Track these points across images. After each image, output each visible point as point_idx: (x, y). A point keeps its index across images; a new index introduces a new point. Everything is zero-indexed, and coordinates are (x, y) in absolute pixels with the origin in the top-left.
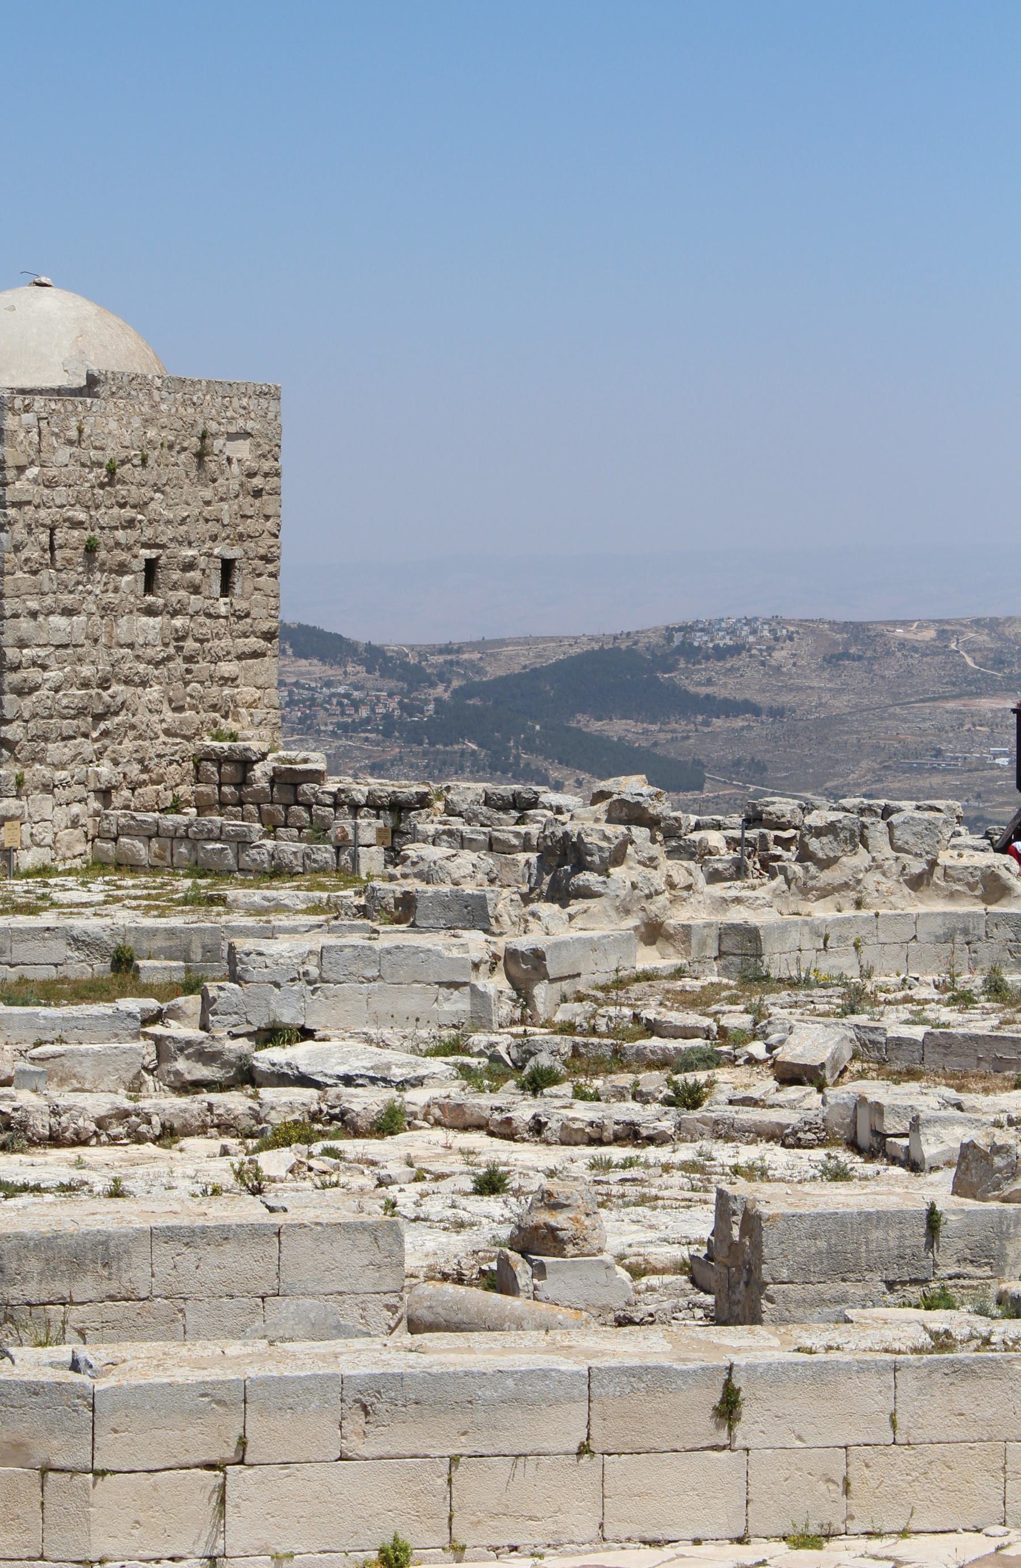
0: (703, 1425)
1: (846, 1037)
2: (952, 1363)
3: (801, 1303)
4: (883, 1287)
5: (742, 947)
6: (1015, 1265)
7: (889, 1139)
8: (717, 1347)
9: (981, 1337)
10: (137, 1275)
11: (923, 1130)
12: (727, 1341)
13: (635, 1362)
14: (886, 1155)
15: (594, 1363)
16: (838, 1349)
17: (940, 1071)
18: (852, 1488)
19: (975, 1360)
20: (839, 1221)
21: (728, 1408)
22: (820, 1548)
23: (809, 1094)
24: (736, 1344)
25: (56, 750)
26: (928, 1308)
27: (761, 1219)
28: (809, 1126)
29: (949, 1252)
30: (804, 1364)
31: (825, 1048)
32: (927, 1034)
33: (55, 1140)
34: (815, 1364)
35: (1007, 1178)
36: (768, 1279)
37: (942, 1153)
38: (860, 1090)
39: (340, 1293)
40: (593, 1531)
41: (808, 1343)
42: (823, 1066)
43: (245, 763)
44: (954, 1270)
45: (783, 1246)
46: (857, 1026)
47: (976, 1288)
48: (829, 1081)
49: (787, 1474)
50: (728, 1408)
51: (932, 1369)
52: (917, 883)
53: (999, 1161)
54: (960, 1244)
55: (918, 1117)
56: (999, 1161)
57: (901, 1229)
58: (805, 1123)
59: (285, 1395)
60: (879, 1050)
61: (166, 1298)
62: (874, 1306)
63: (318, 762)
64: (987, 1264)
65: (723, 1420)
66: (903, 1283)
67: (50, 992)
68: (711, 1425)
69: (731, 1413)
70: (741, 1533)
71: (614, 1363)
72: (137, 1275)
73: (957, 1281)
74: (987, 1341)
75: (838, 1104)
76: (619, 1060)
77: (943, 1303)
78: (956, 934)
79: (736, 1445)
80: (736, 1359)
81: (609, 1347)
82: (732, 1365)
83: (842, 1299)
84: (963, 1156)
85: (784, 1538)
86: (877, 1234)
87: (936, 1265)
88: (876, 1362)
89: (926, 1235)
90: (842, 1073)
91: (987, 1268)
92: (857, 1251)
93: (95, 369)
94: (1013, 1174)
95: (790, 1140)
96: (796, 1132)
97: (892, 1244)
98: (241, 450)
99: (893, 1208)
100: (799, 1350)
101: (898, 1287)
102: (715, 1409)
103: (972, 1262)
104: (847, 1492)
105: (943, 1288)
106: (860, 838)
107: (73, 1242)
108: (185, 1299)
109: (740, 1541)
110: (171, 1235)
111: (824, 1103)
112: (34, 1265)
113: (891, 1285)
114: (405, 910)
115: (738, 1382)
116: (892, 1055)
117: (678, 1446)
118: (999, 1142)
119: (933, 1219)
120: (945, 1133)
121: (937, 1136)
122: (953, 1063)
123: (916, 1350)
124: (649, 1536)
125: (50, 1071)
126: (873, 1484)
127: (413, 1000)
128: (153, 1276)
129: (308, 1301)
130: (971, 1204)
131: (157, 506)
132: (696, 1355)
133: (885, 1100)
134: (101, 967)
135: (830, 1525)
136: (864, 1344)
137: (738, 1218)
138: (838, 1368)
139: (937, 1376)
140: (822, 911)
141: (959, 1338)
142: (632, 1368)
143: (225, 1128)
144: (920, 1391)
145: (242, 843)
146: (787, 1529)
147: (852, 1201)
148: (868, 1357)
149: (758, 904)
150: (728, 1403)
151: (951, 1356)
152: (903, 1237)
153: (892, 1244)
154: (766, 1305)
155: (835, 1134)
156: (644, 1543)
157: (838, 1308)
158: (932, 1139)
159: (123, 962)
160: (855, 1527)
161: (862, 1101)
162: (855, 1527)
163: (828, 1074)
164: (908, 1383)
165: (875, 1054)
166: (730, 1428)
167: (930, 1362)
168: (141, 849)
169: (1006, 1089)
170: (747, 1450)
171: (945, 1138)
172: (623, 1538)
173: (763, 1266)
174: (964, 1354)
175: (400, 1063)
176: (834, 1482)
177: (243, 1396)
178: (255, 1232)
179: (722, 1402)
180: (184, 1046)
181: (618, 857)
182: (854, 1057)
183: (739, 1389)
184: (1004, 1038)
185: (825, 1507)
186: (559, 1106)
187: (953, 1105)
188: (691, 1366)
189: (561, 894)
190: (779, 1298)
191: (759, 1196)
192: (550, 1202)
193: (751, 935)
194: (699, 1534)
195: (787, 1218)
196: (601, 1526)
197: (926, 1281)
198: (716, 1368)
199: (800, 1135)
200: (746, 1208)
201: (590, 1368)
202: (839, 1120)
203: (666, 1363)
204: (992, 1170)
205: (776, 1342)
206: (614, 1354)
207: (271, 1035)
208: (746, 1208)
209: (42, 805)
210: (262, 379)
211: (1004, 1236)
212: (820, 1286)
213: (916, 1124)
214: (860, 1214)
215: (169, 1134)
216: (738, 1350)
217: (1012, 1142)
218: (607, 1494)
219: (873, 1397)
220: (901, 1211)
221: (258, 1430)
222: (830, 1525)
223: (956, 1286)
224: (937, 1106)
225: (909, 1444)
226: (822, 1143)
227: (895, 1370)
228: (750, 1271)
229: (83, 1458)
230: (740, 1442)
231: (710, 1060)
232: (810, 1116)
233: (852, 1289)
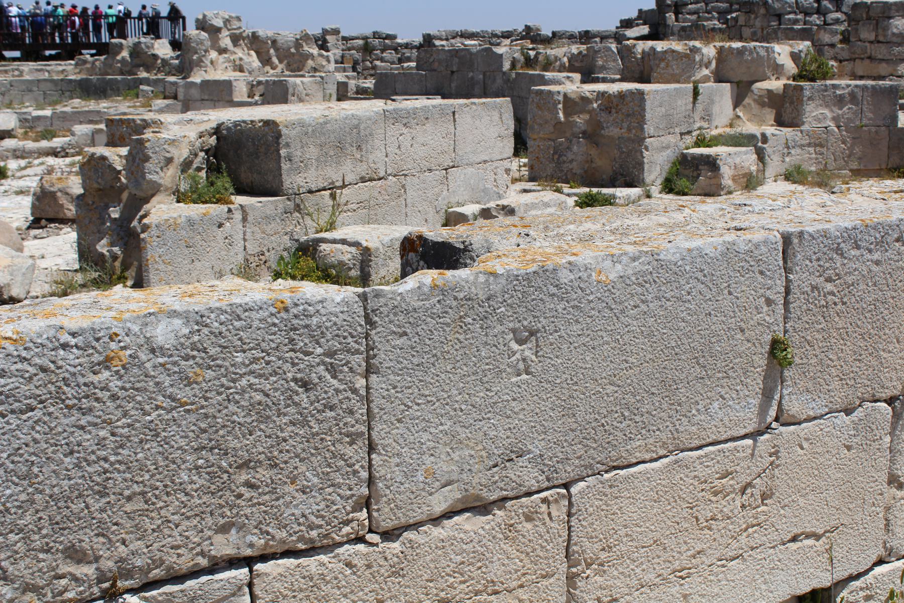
39: (485, 162)
61: (395, 176)
95: (63, 154)
107: (337, 126)
108: (405, 175)
112: (312, 152)
116: (36, 124)
128: (387, 156)
129: (470, 170)
137: (560, 106)
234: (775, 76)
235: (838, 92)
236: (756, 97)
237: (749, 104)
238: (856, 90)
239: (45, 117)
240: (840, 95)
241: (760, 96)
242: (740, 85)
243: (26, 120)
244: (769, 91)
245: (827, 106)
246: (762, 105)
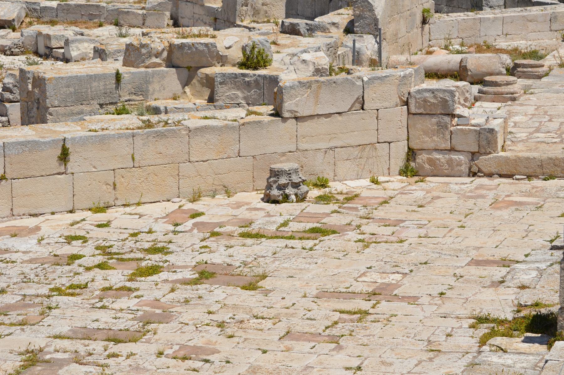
0: (54, 164)
1: (22, 7)
2: (156, 132)
3: (64, 115)
4: (98, 107)
6: (153, 94)
7: (54, 50)
8: (55, 132)
9: (164, 121)
11: (71, 45)
12: (58, 129)
13: (22, 139)
14: (53, 57)
15: (5, 140)
16: (106, 129)
17: (65, 21)
18: (116, 187)
19: (166, 131)
21: (64, 156)
22: (105, 212)
23: (9, 32)
24: (63, 130)
26: (118, 114)
27: (45, 80)
28: (17, 46)
29: (125, 90)
30: (95, 136)
31: (14, 12)
32: (59, 5)
34: (100, 136)
35: (147, 58)
36: (50, 106)
37: (80, 54)
38: (38, 29)
40: (8, 212)
41: (93, 128)
42: (14, 20)
44: (127, 98)
45: (55, 91)
46: (26, 2)
47: (135, 104)
48: (17, 27)
49: (90, 183)
50: (64, 156)
51: (148, 135)
53: (144, 51)
54: (130, 87)
55: (68, 39)
56: (144, 51)
57: (105, 82)
58: (15, 45)
60: (37, 12)
62: (95, 115)
64: (141, 94)
65: (62, 162)
66: (107, 104)
68: (57, 164)
69: (65, 158)
70: (71, 208)
71: (13, 140)
73: (129, 102)
74: (166, 123)
75: (28, 36)
77: (124, 112)
79: (68, 172)
80: (66, 135)
81: (8, 134)
82: (65, 138)
83: (81, 113)
84: (127, 49)
85: (90, 210)
86: (95, 84)
87: (120, 96)
88: (125, 134)
89: (116, 83)
90: (22, 23)
91: (141, 96)
92: (87, 92)
94: (150, 56)
96: (11, 49)
97: (101, 88)
99: (101, 73)
100: (90, 131)
101: (105, 106)
102: (59, 157)
103: (135, 94)
104: (114, 188)
105: (124, 106)
109: (71, 212)
111: (22, 35)
113: (101, 105)
115: (68, 145)
116: (43, 14)
117: (43, 174)
118: (144, 43)
119: (118, 77)
120: (81, 46)
121: (77, 47)
122: (71, 17)
123: (139, 128)
124: (33, 212)
126: (126, 184)
130: (132, 70)
132: (47, 135)
133: (51, 33)
135: (108, 202)
136: (118, 127)
137: (31, 81)
138: (109, 137)
139: (150, 138)
141: (154, 122)
142: (22, 142)
144: (144, 145)
146: (91, 206)
147: (82, 70)
148: (121, 131)
150: (64, 154)
151: (153, 129)
152: (105, 85)
153: (101, 88)
154: (49, 117)
155: (28, 49)
156: (31, 215)
157: (80, 116)
158: (75, 49)
160: (119, 203)
161: (39, 34)
162: (119, 203)
163: (16, 24)
164: (139, 141)
165: (35, 14)
166: (65, 165)
167: (148, 132)
169: (95, 27)
170: (73, 174)
171: (81, 48)
172: (21, 214)
173: (47, 100)
174: (160, 128)
176: (109, 185)
179: (61, 154)
182: (27, 16)
183: (69, 148)
184: (93, 5)
185: (108, 197)
187: (79, 34)
188: (47, 140)
190: (54, 114)
191: (40, 71)
194: (54, 210)
195: (57, 79)
196: (12, 210)
197: (116, 103)
198: (58, 140)
199: (12, 50)
200: (34, 76)
201: (4, 143)
202: (30, 43)
203: (37, 139)
204: (141, 55)
205: (79, 128)
206: (12, 137)
208: (34, 76)
211: (148, 82)
212: (72, 107)
213: (67, 42)
214: (87, 76)
216: (64, 132)
217: (149, 42)
218: (13, 196)
220: (105, 74)
222: (108, 202)
223: (128, 104)
224: (72, 34)
225: (140, 167)
226: (23, 53)
227: (133, 136)
228: (38, 103)
230: (69, 171)
232: (16, 41)
233: (84, 108)
234: (221, 64)
235: (247, 79)
236: (199, 79)
237: (194, 83)
238: (259, 78)
239: (51, 8)
240: (248, 82)
241: (201, 78)
242: (191, 69)
243: (35, 10)
244: (207, 75)
245: (238, 89)
246: (203, 85)
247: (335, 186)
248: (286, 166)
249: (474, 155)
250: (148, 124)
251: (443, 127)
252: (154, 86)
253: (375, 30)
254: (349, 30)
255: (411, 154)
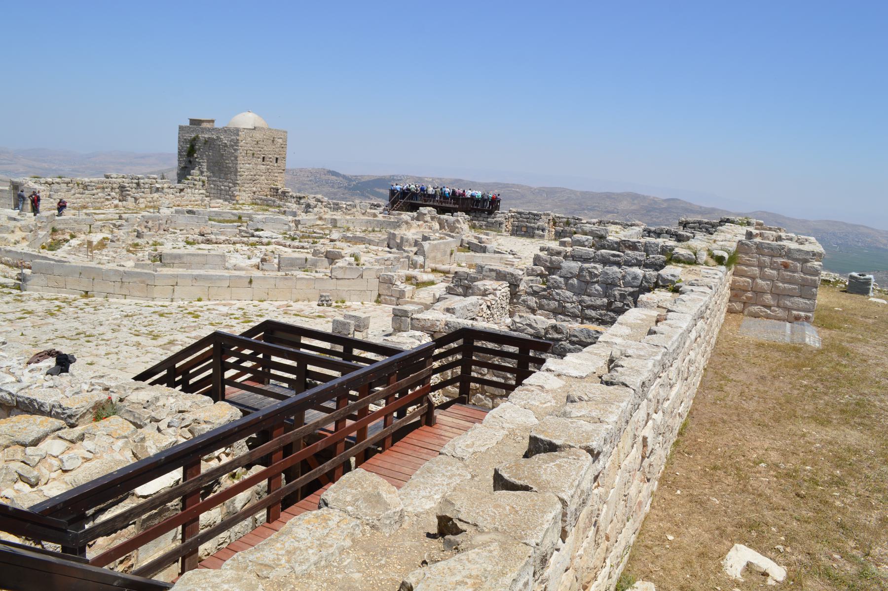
5: (334, 223)
10: (185, 260)
20: (292, 259)
21: (251, 282)
25: (246, 185)
33: (216, 243)
43: (278, 190)
50: (251, 282)
52: (363, 214)
59: (183, 276)
63: (290, 190)
67: (227, 221)
72: (185, 260)
76: (309, 237)
78: (368, 222)
93: (256, 125)
98: (280, 141)
106: (355, 206)
110: (190, 255)
114: (285, 213)
119: (306, 259)
125: (222, 233)
127: (279, 226)
131: (265, 148)
134: (236, 218)
140: (348, 217)
143: (243, 243)
145: (274, 202)
149: (338, 215)
159: (240, 218)
168: (259, 201)
175: (274, 235)
177: (177, 276)
178: (203, 255)
180: (243, 231)
181: (315, 207)
185: (264, 296)
186: (296, 243)
189: (306, 212)
192: (266, 255)
193: (335, 220)
207: (257, 230)
209: (244, 194)
210: (284, 130)
215: (234, 243)
219: (273, 282)
221: (179, 281)
229: (152, 283)
231: (322, 238)
247: (348, 303)
248: (324, 294)
249: (398, 298)
250: (286, 275)
251: (389, 288)
252: (319, 264)
253: (423, 254)
254: (416, 254)
255: (379, 295)
